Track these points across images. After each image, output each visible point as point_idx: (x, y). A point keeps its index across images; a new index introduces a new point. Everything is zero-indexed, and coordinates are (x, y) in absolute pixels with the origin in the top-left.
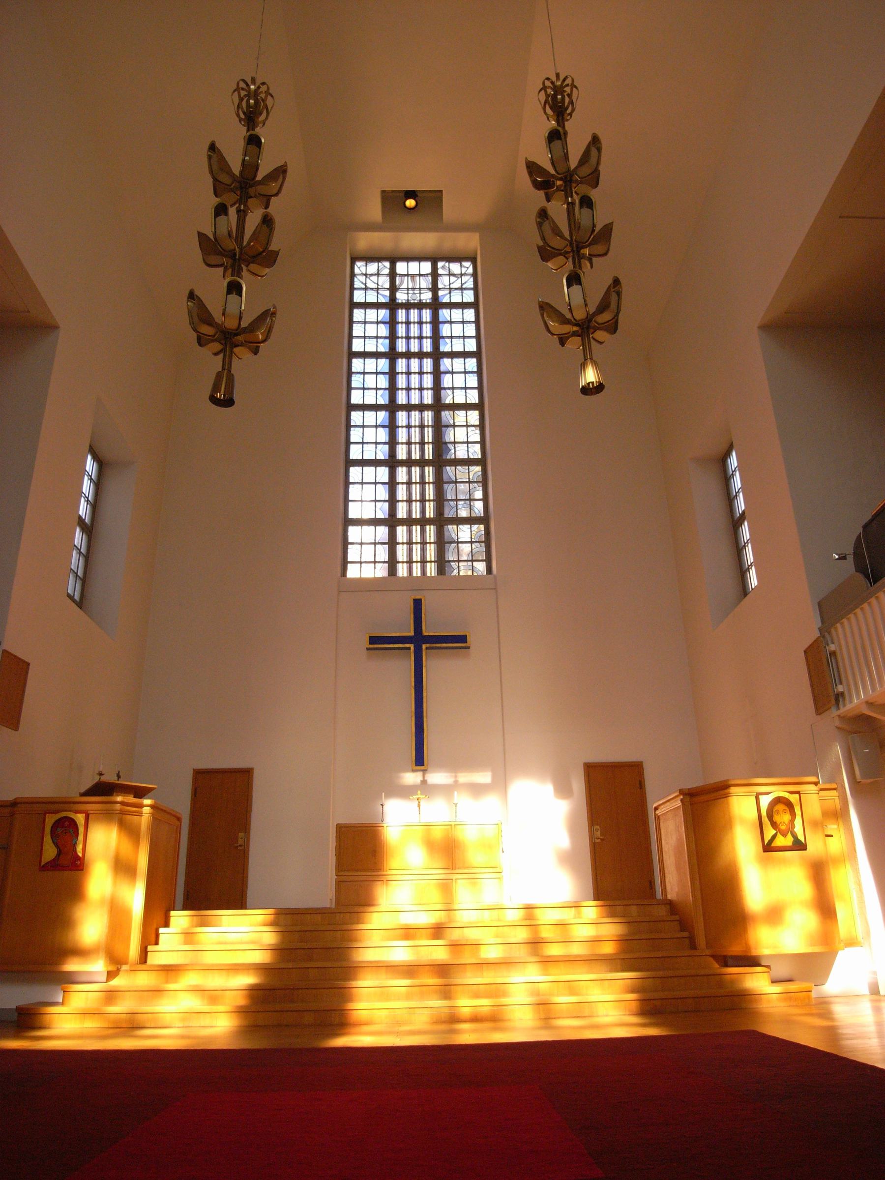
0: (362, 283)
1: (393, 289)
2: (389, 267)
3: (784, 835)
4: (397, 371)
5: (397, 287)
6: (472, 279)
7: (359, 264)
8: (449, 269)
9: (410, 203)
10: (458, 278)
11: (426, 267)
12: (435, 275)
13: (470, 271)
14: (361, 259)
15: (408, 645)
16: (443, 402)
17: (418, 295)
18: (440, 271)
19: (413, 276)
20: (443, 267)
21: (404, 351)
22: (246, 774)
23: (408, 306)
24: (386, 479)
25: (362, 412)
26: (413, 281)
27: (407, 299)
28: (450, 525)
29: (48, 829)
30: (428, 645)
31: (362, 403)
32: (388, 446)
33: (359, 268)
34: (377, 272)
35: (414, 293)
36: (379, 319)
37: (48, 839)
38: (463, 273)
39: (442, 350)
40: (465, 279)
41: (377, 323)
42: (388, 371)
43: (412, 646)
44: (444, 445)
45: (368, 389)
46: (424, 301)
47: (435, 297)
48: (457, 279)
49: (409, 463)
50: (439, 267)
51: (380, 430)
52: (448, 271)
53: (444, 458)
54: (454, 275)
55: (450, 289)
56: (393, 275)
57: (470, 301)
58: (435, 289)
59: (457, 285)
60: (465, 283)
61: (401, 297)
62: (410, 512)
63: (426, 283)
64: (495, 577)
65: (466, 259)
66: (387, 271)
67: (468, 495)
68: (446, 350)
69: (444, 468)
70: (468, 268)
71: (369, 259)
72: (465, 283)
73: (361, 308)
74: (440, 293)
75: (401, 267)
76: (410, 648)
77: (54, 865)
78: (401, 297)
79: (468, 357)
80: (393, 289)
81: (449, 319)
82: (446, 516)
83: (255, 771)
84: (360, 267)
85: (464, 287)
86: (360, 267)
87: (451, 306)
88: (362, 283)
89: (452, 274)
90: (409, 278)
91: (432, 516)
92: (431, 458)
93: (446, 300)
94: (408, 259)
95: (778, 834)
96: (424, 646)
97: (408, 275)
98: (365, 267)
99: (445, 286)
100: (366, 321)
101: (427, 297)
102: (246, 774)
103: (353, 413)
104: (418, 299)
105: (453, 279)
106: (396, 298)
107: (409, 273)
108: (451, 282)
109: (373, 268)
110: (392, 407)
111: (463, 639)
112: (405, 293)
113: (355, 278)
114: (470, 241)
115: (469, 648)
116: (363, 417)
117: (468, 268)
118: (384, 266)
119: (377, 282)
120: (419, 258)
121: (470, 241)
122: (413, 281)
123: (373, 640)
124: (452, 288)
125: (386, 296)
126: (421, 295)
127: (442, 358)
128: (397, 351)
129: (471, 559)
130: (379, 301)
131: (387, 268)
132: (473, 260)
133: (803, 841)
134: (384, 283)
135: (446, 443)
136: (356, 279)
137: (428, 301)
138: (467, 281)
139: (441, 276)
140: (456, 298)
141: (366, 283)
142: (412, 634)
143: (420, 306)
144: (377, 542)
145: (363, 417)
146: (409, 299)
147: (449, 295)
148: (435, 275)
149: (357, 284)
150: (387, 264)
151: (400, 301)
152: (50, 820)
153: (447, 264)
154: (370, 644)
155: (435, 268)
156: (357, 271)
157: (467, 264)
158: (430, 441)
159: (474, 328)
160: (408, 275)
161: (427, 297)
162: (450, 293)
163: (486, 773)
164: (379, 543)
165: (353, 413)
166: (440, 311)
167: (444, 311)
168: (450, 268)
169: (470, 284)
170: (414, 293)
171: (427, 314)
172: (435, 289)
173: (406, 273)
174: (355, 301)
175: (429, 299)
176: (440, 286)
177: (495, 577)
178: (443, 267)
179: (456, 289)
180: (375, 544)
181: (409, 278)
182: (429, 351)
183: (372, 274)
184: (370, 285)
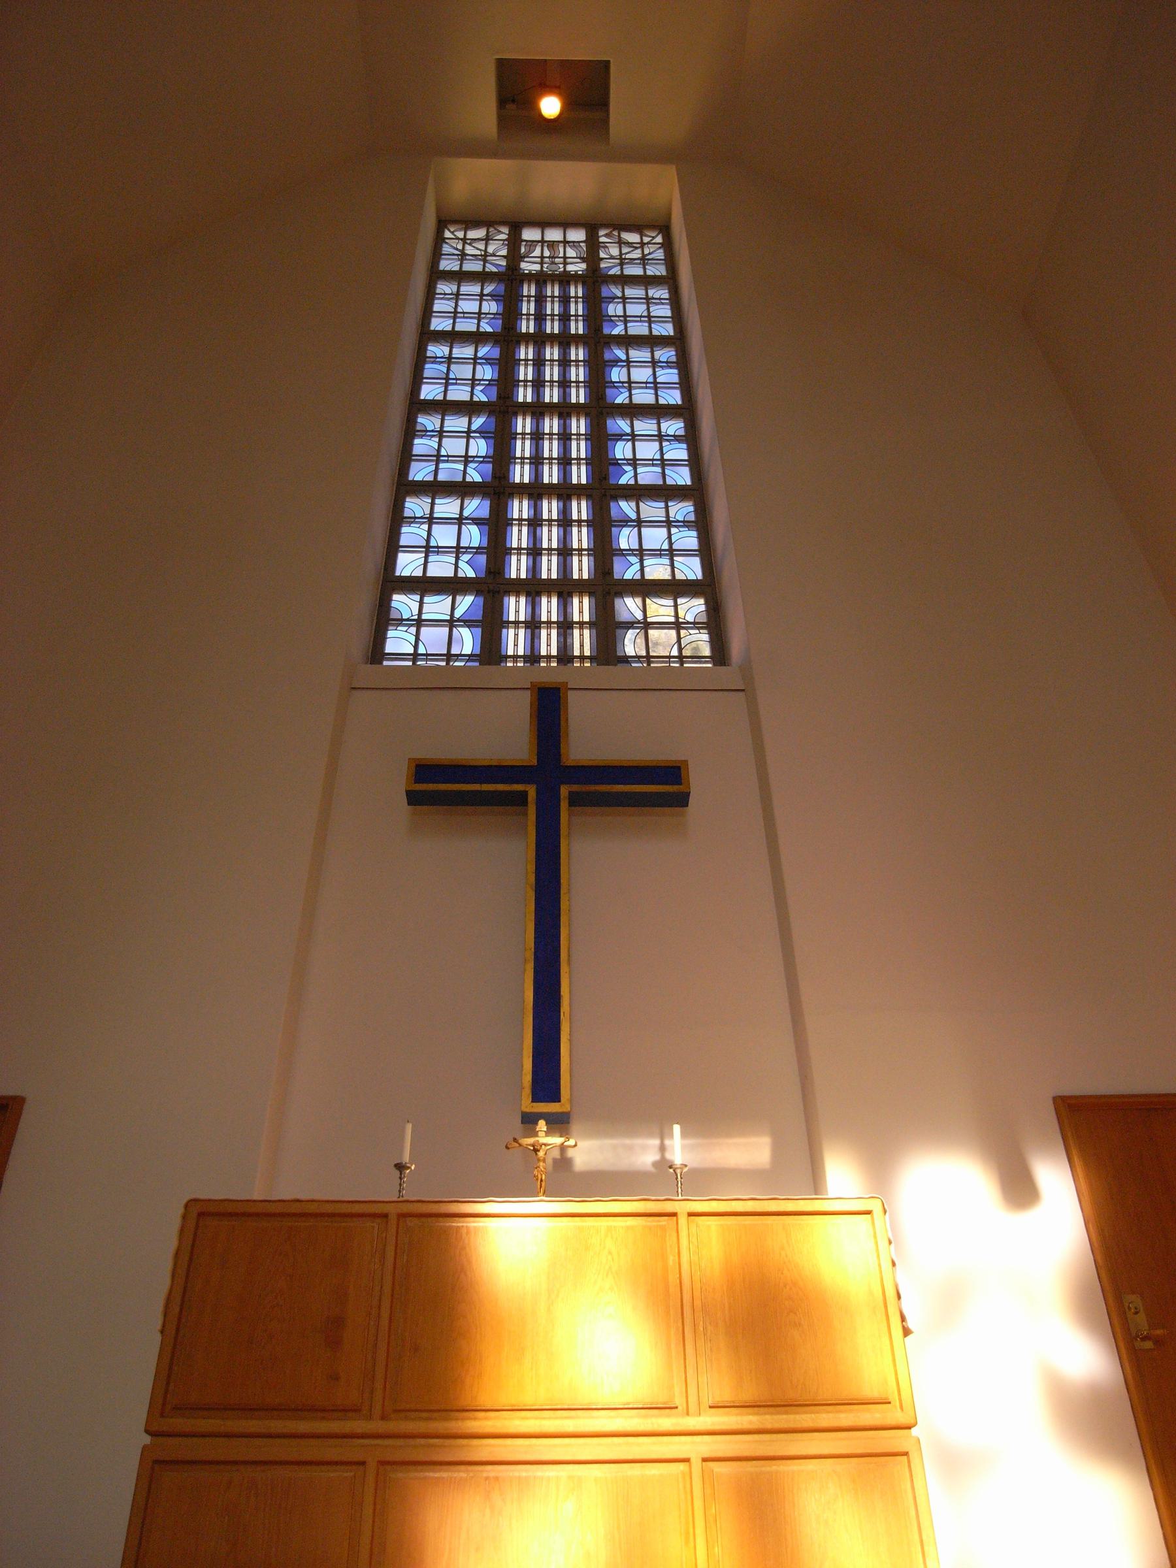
0: (457, 249)
9: (550, 106)
11: (577, 235)
13: (659, 239)
17: (561, 266)
20: (606, 235)
28: (628, 596)
30: (575, 788)
32: (491, 465)
39: (606, 331)
43: (532, 791)
44: (611, 468)
53: (612, 482)
54: (629, 244)
59: (637, 254)
60: (650, 254)
65: (652, 227)
72: (650, 254)
75: (529, 234)
76: (524, 794)
82: (616, 577)
83: (26, 1107)
89: (624, 243)
91: (585, 576)
92: (584, 481)
94: (543, 225)
96: (564, 791)
98: (463, 232)
99: (612, 256)
105: (625, 250)
111: (673, 773)
113: (445, 245)
115: (682, 800)
118: (500, 231)
119: (483, 249)
123: (424, 771)
150: (506, 230)
153: (616, 233)
154: (418, 780)
156: (447, 234)
163: (753, 1140)
175: (582, 271)
177: (746, 670)
183: (475, 239)
184: (469, 250)
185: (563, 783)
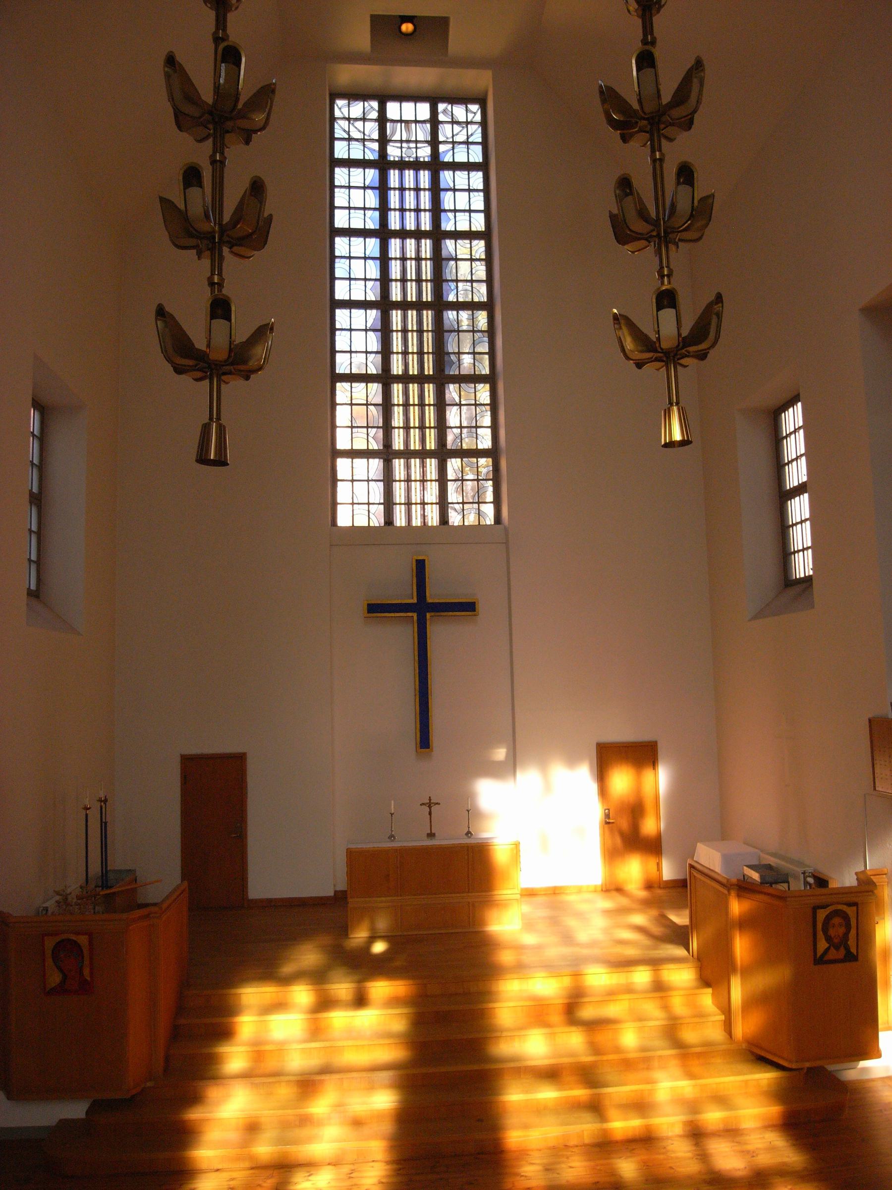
1: (383, 140)
2: (377, 109)
3: (837, 948)
4: (390, 256)
5: (388, 138)
6: (480, 130)
7: (340, 103)
8: (452, 114)
10: (463, 127)
11: (424, 111)
12: (434, 122)
13: (478, 118)
14: (343, 96)
15: (410, 614)
16: (445, 299)
17: (414, 150)
18: (441, 117)
19: (407, 122)
20: (445, 111)
21: (398, 228)
22: (238, 761)
23: (402, 165)
24: (379, 400)
25: (349, 310)
26: (408, 130)
27: (400, 155)
29: (49, 953)
30: (433, 614)
31: (348, 299)
33: (340, 109)
34: (362, 115)
35: (409, 148)
36: (367, 184)
37: (49, 962)
38: (469, 120)
40: (472, 128)
41: (364, 188)
42: (379, 256)
43: (415, 615)
45: (356, 279)
46: (422, 160)
47: (435, 153)
48: (461, 128)
49: (405, 379)
50: (439, 111)
51: (370, 334)
52: (451, 117)
54: (458, 123)
55: (453, 143)
56: (382, 120)
57: (477, 161)
58: (434, 142)
59: (461, 138)
60: (472, 135)
61: (393, 152)
62: (407, 442)
63: (422, 133)
64: (506, 530)
65: (473, 101)
66: (374, 115)
67: (474, 421)
68: (448, 229)
69: (446, 385)
70: (475, 113)
71: (353, 96)
72: (472, 135)
73: (344, 166)
74: (442, 148)
75: (393, 109)
76: (413, 616)
77: (61, 990)
78: (393, 152)
79: (475, 239)
80: (383, 140)
81: (452, 185)
82: (449, 447)
83: (248, 755)
84: (341, 107)
85: (470, 140)
86: (341, 107)
87: (455, 166)
88: (345, 131)
90: (403, 124)
92: (431, 373)
93: (448, 158)
95: (832, 948)
97: (401, 121)
98: (347, 108)
99: (447, 138)
100: (351, 185)
101: (425, 153)
102: (238, 761)
103: (338, 312)
104: (415, 155)
105: (457, 128)
106: (387, 153)
107: (403, 119)
108: (454, 134)
109: (357, 109)
110: (384, 305)
111: (469, 607)
112: (398, 147)
114: (482, 79)
116: (350, 317)
117: (475, 113)
118: (372, 107)
119: (362, 131)
120: (415, 98)
121: (482, 79)
122: (408, 130)
124: (456, 142)
125: (374, 150)
126: (418, 150)
127: (445, 239)
128: (390, 228)
129: (477, 501)
130: (367, 158)
131: (374, 110)
132: (482, 102)
133: (855, 954)
134: (371, 131)
135: (449, 353)
136: (336, 126)
137: (426, 159)
138: (474, 132)
139: (443, 124)
140: (461, 156)
141: (349, 131)
142: (415, 601)
143: (417, 165)
144: (370, 479)
145: (350, 317)
146: (404, 155)
147: (452, 151)
148: (434, 122)
149: (338, 133)
150: (375, 104)
151: (392, 159)
152: (50, 943)
153: (449, 107)
155: (434, 112)
156: (337, 113)
157: (474, 108)
158: (430, 351)
159: (482, 198)
160: (401, 121)
161: (425, 153)
162: (453, 148)
164: (372, 480)
165: (338, 312)
166: (441, 173)
167: (446, 172)
168: (453, 113)
169: (478, 138)
170: (409, 148)
171: (425, 177)
172: (434, 142)
173: (399, 119)
174: (336, 156)
175: (428, 156)
176: (441, 138)
178: (445, 111)
179: (460, 143)
180: (368, 481)
181: (403, 124)
182: (428, 229)
184: (355, 134)
185: (428, 612)
